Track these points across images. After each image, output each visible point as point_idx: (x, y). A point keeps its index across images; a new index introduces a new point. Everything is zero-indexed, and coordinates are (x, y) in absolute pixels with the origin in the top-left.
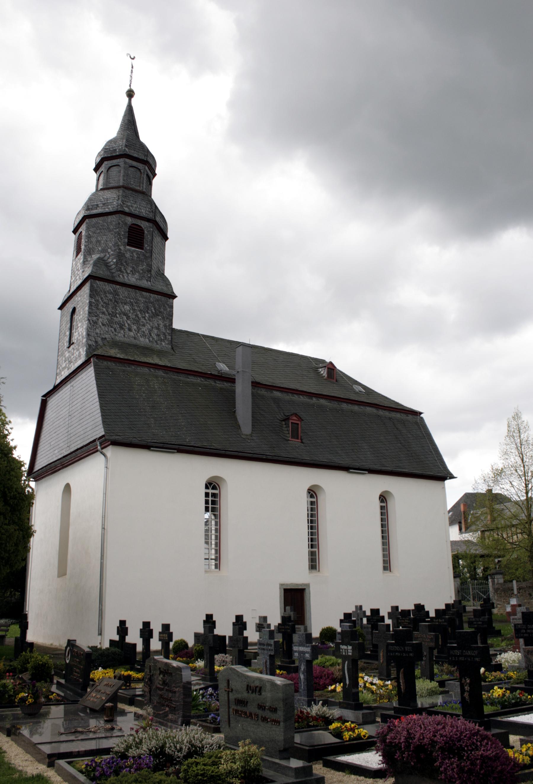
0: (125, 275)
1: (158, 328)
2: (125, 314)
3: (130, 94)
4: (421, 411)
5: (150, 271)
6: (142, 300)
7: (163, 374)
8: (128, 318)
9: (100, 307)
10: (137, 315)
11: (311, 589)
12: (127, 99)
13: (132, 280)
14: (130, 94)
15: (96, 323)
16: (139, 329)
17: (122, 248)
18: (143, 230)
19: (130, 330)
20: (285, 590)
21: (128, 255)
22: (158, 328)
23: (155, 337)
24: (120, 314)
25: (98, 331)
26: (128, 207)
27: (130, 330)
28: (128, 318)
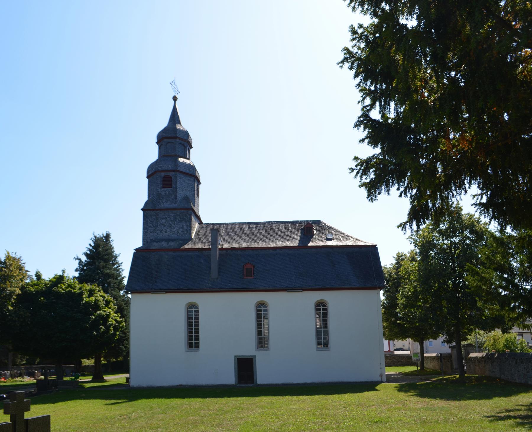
0: (162, 204)
1: (183, 228)
2: (163, 225)
3: (175, 99)
4: (375, 244)
5: (176, 198)
6: (172, 215)
7: (174, 254)
8: (165, 226)
9: (149, 224)
10: (170, 224)
11: (257, 358)
12: (173, 102)
13: (167, 205)
14: (175, 99)
15: (147, 232)
16: (171, 231)
17: (159, 190)
18: (171, 178)
19: (166, 232)
20: (252, 359)
21: (163, 193)
22: (183, 228)
23: (181, 233)
24: (160, 225)
25: (148, 236)
26: (161, 167)
27: (166, 232)
28: (165, 226)
